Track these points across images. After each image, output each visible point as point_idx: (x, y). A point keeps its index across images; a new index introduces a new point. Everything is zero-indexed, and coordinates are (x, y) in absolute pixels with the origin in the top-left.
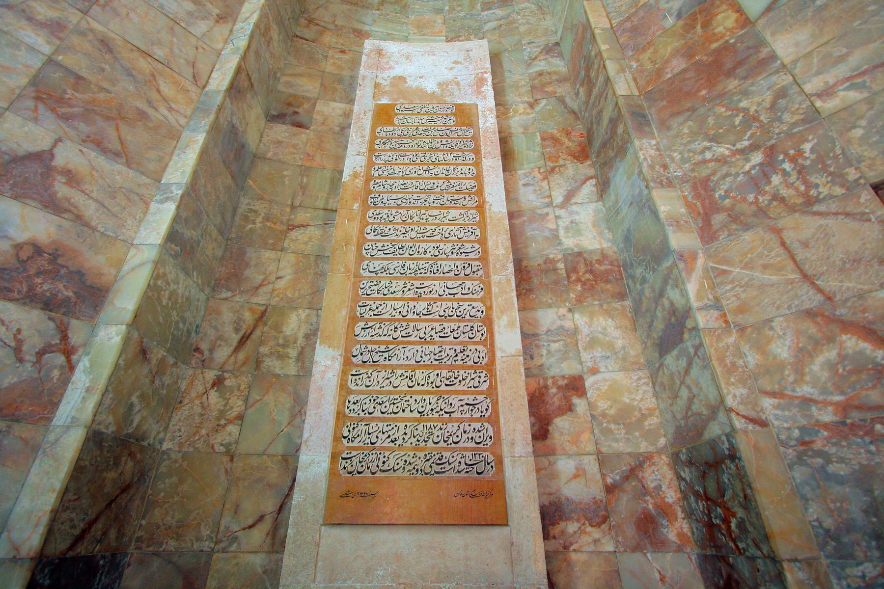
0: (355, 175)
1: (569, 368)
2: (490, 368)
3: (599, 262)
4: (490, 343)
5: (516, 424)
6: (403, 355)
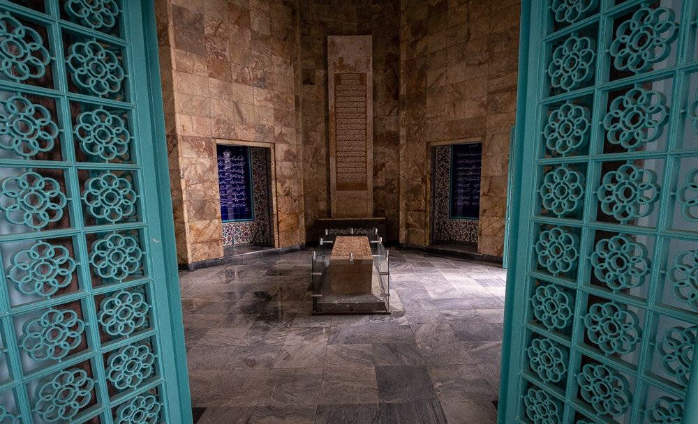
0: (332, 107)
1: (382, 161)
2: (366, 162)
3: (394, 135)
4: (366, 157)
5: (370, 174)
6: (348, 159)
